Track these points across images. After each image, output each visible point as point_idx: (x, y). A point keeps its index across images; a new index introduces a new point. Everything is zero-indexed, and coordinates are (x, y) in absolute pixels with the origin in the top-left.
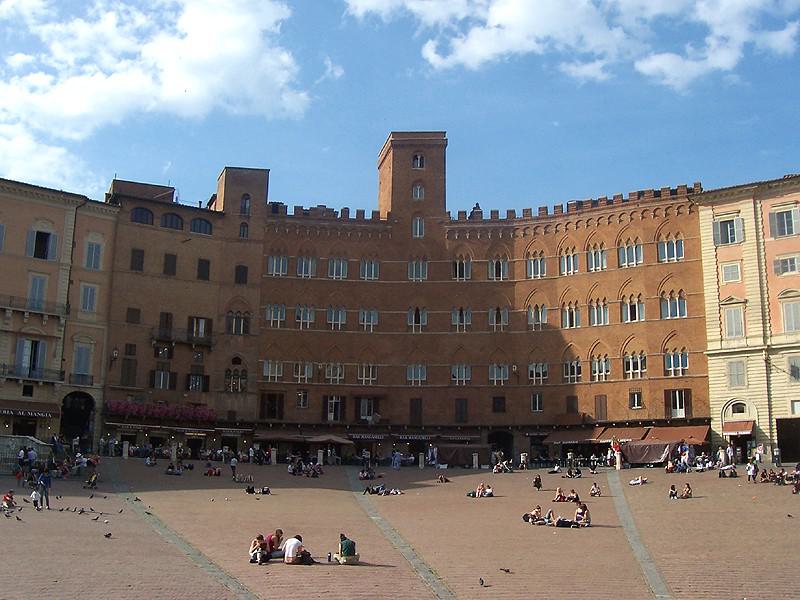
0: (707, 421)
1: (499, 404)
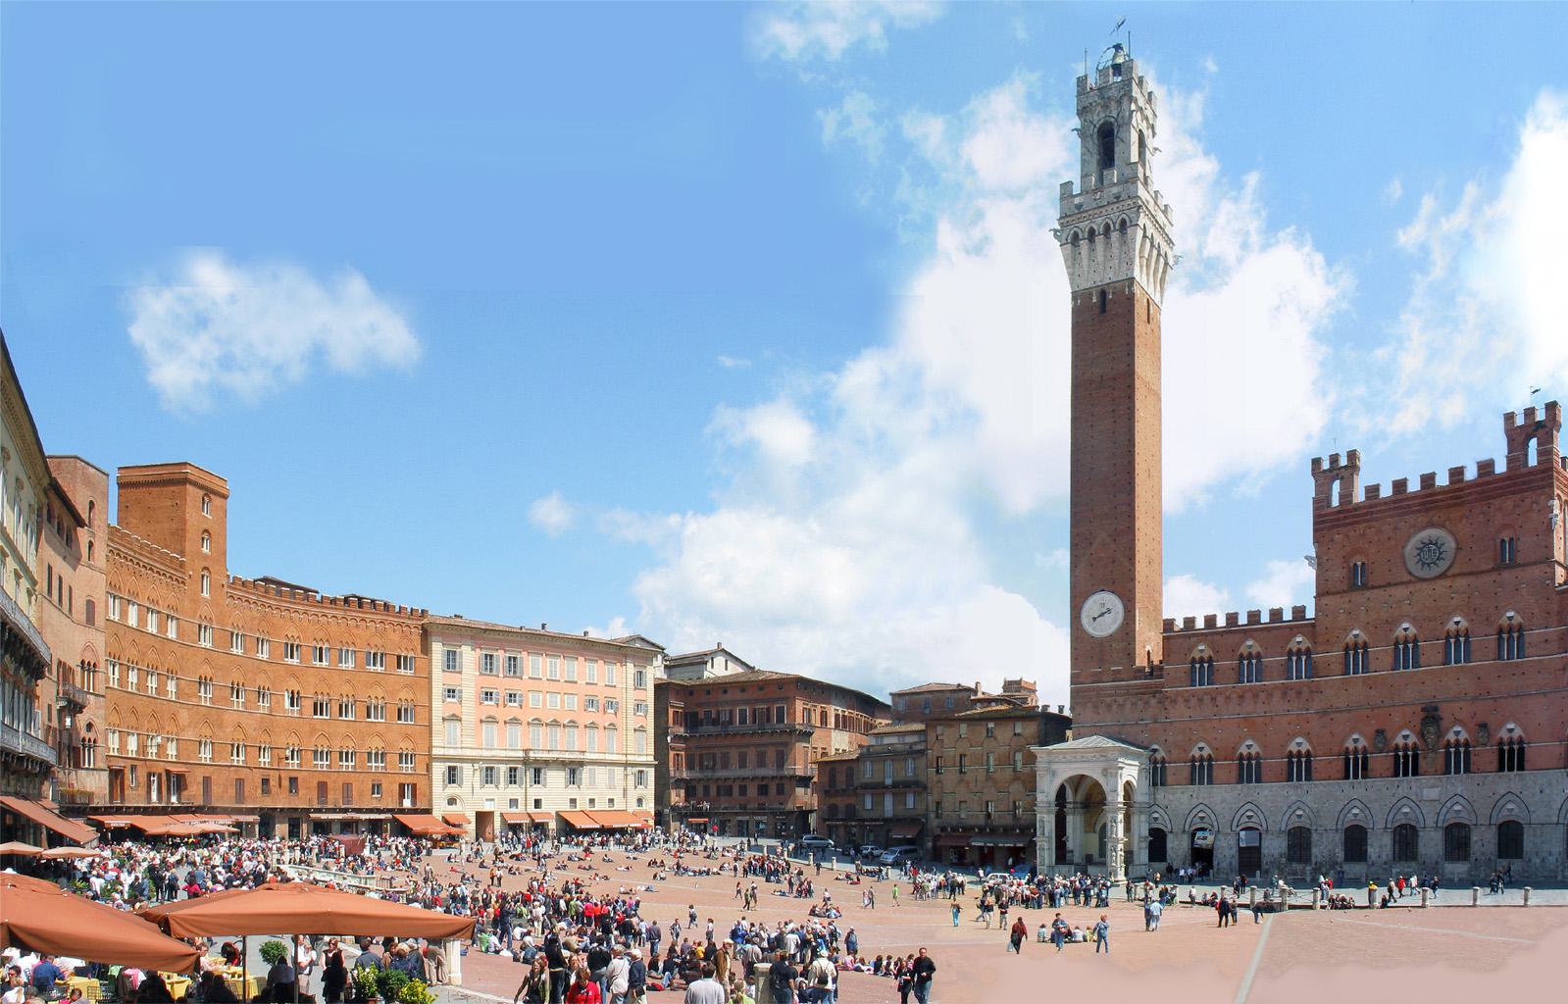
0: (428, 811)
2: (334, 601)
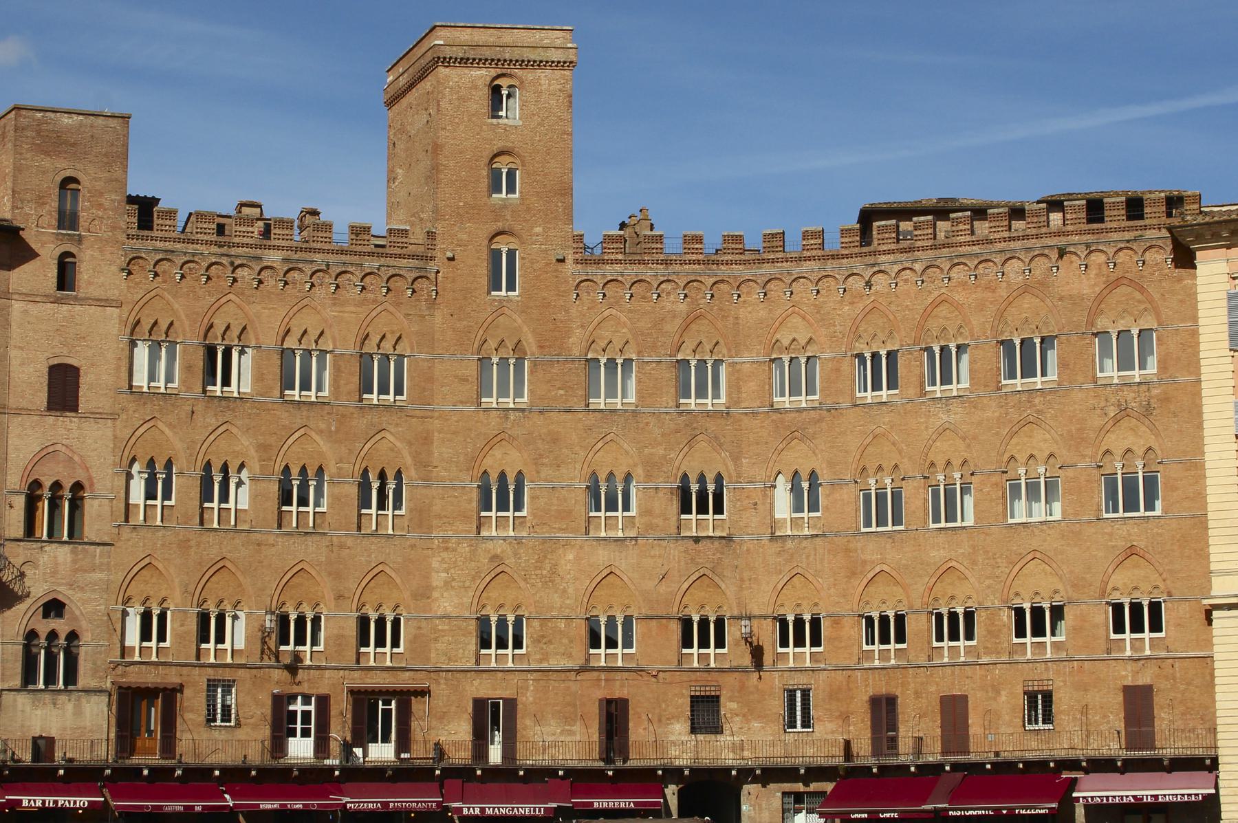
0: (1209, 765)
1: (705, 713)
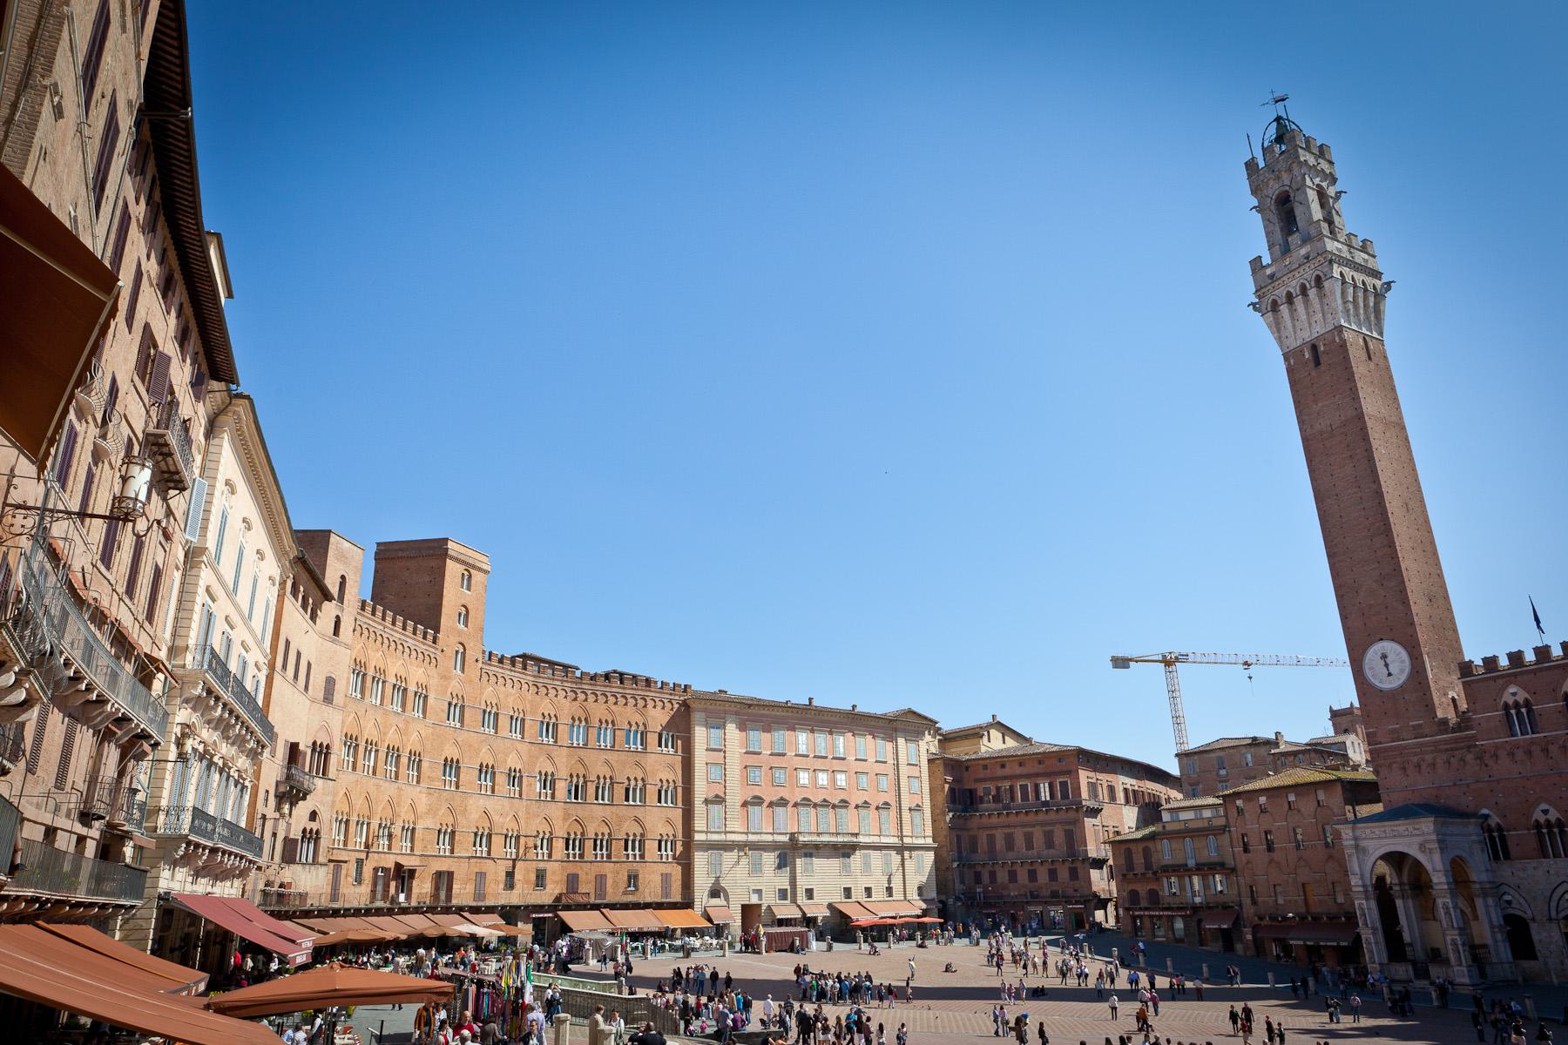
0: (687, 904)
2: (594, 678)
